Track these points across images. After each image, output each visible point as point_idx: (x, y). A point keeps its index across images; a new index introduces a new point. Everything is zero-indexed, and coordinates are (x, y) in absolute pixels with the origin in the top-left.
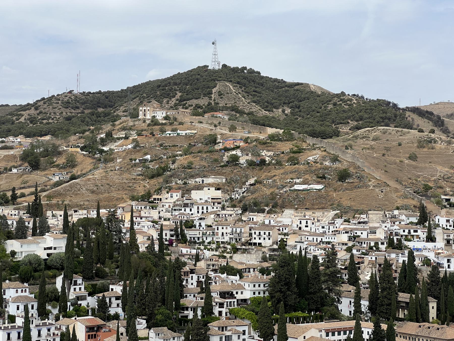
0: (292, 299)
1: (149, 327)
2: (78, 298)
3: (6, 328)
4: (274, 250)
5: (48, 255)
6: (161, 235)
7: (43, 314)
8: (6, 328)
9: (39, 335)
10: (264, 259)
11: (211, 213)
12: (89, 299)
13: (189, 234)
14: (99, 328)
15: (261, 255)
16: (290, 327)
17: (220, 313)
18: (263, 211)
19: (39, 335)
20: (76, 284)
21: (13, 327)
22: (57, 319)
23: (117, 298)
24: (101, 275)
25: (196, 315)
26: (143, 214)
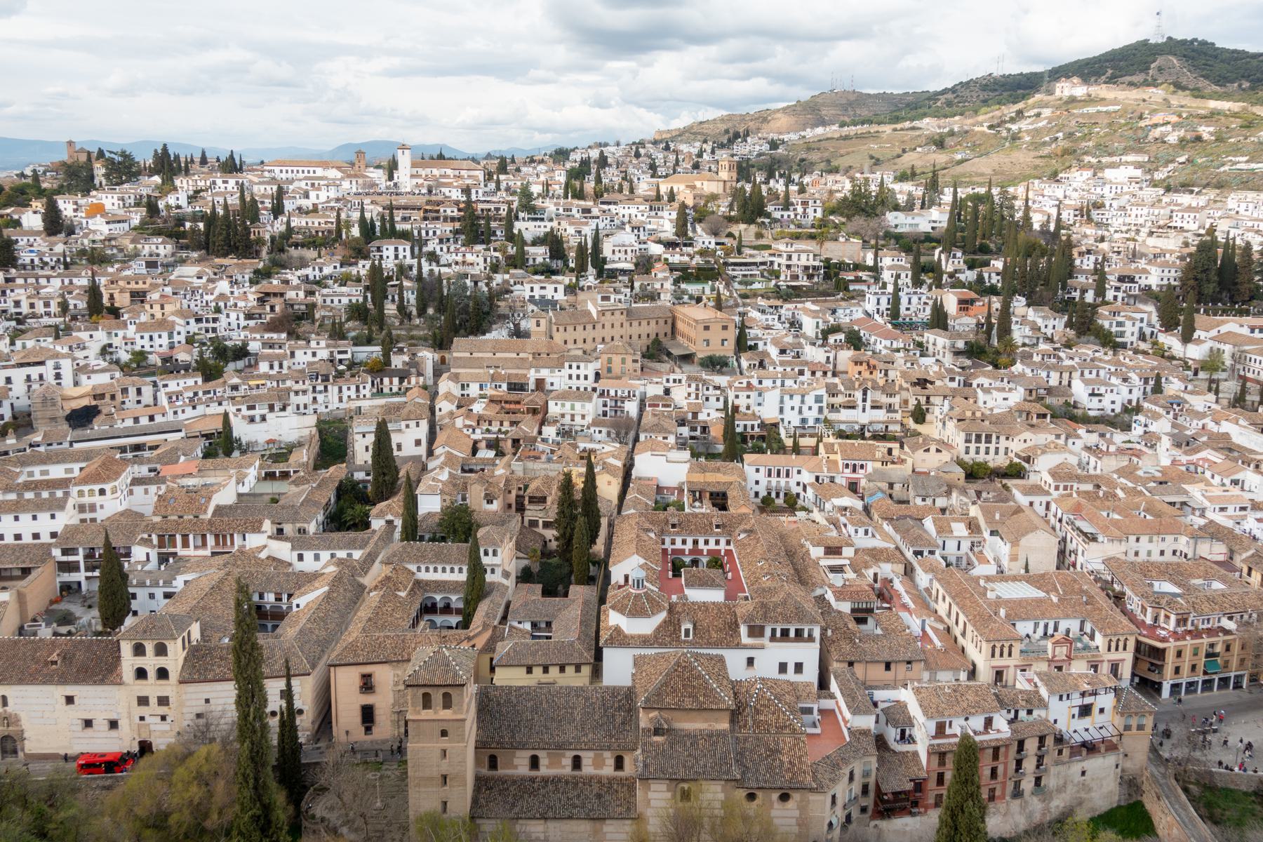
0: (1210, 288)
1: (1028, 305)
2: (956, 271)
3: (876, 294)
4: (1199, 235)
5: (933, 228)
6: (1059, 214)
7: (917, 283)
8: (876, 294)
9: (909, 303)
10: (1186, 244)
11: (1126, 193)
12: (968, 273)
13: (1095, 214)
14: (972, 302)
15: (1181, 240)
16: (1200, 318)
17: (1115, 298)
18: (1192, 192)
19: (909, 303)
20: (954, 257)
21: (883, 293)
22: (930, 289)
23: (998, 274)
24: (984, 250)
25: (1082, 298)
26: (1046, 192)
